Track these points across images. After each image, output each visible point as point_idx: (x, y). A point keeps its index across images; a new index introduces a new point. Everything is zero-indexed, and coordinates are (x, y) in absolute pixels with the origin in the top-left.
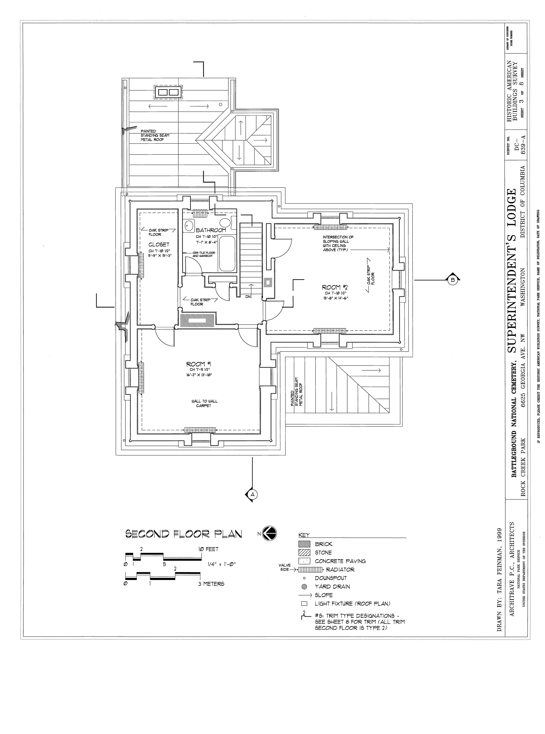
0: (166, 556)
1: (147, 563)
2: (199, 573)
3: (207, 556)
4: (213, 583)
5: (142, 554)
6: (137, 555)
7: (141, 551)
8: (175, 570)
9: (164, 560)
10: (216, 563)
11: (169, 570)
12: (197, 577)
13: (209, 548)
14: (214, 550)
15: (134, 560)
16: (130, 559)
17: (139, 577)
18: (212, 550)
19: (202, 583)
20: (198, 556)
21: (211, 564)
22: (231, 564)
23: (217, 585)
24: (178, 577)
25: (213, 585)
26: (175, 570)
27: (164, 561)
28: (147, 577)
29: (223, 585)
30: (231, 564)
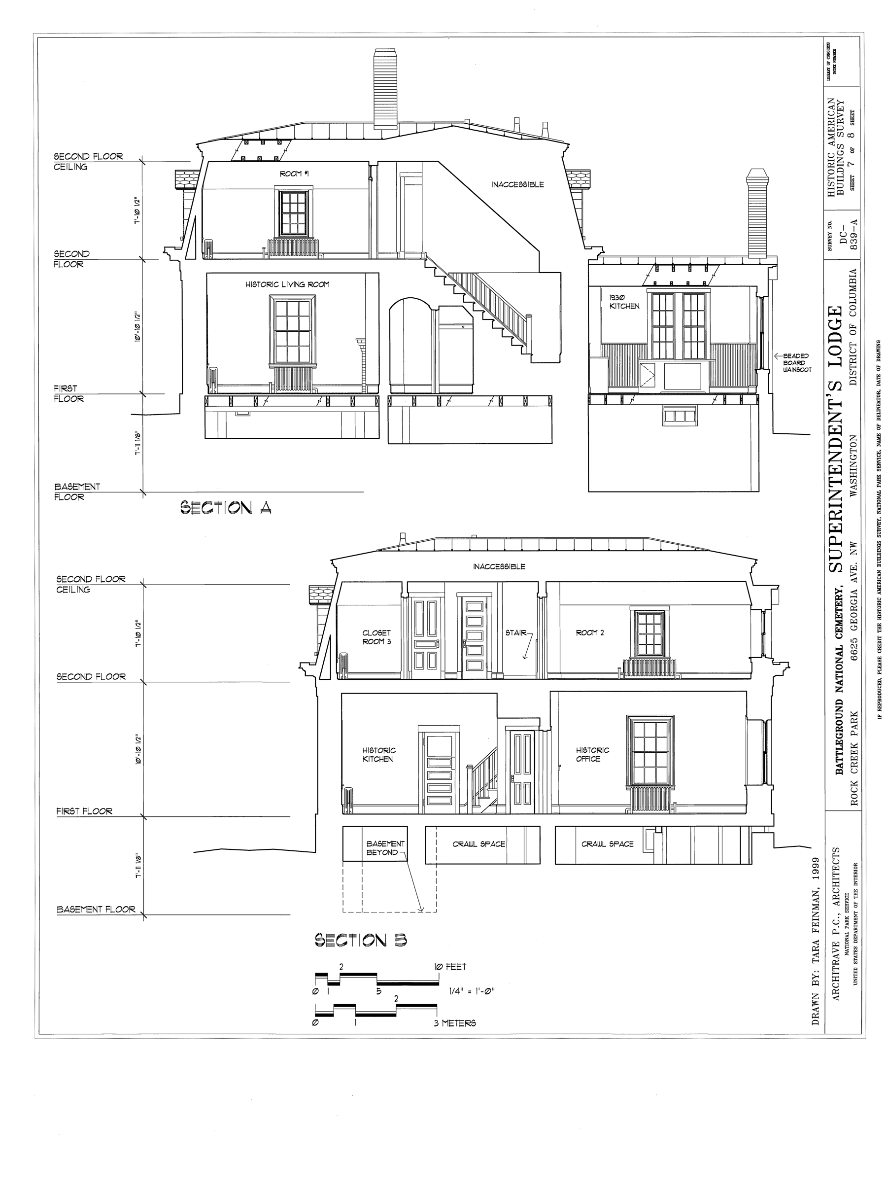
0: (381, 978)
1: (349, 990)
2: (435, 1005)
3: (448, 978)
4: (458, 1022)
5: (341, 974)
6: (334, 976)
7: (341, 969)
8: (395, 1001)
9: (379, 984)
10: (462, 989)
11: (386, 1000)
12: (431, 1011)
13: (450, 965)
14: (458, 968)
15: (329, 984)
16: (323, 982)
17: (338, 1012)
18: (456, 968)
19: (440, 1022)
20: (432, 976)
21: (455, 991)
22: (488, 991)
23: (464, 1024)
24: (401, 1012)
25: (458, 1024)
26: (395, 1001)
27: (379, 987)
28: (351, 1012)
29: (474, 1024)
30: (488, 991)
